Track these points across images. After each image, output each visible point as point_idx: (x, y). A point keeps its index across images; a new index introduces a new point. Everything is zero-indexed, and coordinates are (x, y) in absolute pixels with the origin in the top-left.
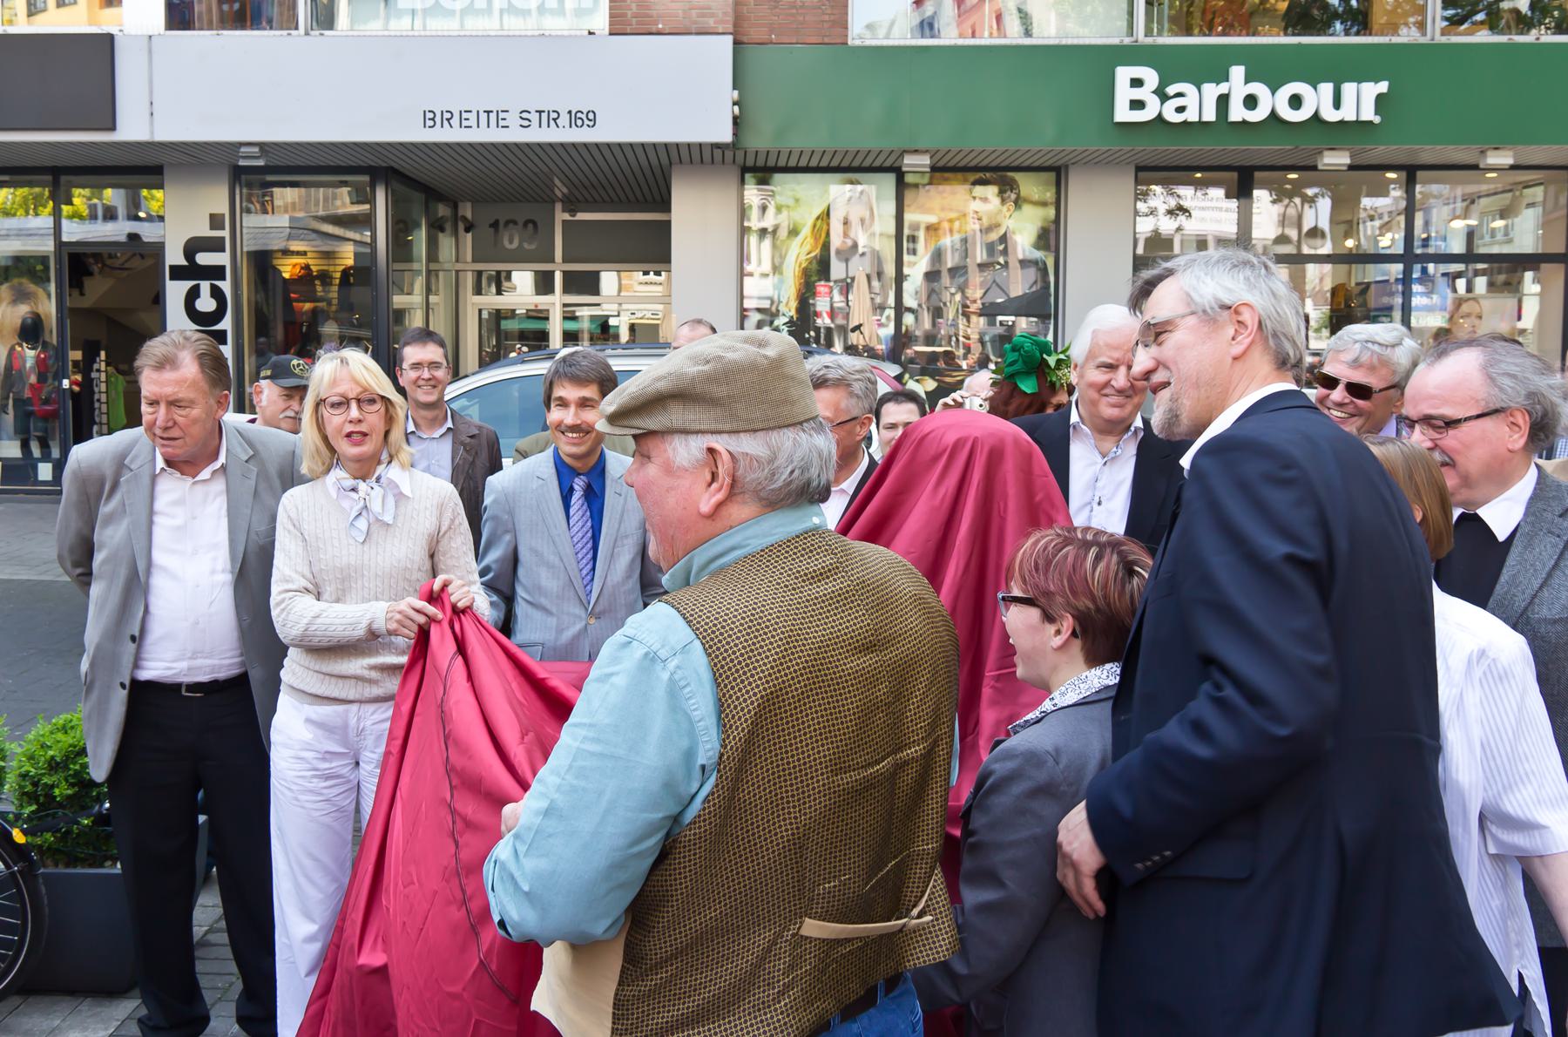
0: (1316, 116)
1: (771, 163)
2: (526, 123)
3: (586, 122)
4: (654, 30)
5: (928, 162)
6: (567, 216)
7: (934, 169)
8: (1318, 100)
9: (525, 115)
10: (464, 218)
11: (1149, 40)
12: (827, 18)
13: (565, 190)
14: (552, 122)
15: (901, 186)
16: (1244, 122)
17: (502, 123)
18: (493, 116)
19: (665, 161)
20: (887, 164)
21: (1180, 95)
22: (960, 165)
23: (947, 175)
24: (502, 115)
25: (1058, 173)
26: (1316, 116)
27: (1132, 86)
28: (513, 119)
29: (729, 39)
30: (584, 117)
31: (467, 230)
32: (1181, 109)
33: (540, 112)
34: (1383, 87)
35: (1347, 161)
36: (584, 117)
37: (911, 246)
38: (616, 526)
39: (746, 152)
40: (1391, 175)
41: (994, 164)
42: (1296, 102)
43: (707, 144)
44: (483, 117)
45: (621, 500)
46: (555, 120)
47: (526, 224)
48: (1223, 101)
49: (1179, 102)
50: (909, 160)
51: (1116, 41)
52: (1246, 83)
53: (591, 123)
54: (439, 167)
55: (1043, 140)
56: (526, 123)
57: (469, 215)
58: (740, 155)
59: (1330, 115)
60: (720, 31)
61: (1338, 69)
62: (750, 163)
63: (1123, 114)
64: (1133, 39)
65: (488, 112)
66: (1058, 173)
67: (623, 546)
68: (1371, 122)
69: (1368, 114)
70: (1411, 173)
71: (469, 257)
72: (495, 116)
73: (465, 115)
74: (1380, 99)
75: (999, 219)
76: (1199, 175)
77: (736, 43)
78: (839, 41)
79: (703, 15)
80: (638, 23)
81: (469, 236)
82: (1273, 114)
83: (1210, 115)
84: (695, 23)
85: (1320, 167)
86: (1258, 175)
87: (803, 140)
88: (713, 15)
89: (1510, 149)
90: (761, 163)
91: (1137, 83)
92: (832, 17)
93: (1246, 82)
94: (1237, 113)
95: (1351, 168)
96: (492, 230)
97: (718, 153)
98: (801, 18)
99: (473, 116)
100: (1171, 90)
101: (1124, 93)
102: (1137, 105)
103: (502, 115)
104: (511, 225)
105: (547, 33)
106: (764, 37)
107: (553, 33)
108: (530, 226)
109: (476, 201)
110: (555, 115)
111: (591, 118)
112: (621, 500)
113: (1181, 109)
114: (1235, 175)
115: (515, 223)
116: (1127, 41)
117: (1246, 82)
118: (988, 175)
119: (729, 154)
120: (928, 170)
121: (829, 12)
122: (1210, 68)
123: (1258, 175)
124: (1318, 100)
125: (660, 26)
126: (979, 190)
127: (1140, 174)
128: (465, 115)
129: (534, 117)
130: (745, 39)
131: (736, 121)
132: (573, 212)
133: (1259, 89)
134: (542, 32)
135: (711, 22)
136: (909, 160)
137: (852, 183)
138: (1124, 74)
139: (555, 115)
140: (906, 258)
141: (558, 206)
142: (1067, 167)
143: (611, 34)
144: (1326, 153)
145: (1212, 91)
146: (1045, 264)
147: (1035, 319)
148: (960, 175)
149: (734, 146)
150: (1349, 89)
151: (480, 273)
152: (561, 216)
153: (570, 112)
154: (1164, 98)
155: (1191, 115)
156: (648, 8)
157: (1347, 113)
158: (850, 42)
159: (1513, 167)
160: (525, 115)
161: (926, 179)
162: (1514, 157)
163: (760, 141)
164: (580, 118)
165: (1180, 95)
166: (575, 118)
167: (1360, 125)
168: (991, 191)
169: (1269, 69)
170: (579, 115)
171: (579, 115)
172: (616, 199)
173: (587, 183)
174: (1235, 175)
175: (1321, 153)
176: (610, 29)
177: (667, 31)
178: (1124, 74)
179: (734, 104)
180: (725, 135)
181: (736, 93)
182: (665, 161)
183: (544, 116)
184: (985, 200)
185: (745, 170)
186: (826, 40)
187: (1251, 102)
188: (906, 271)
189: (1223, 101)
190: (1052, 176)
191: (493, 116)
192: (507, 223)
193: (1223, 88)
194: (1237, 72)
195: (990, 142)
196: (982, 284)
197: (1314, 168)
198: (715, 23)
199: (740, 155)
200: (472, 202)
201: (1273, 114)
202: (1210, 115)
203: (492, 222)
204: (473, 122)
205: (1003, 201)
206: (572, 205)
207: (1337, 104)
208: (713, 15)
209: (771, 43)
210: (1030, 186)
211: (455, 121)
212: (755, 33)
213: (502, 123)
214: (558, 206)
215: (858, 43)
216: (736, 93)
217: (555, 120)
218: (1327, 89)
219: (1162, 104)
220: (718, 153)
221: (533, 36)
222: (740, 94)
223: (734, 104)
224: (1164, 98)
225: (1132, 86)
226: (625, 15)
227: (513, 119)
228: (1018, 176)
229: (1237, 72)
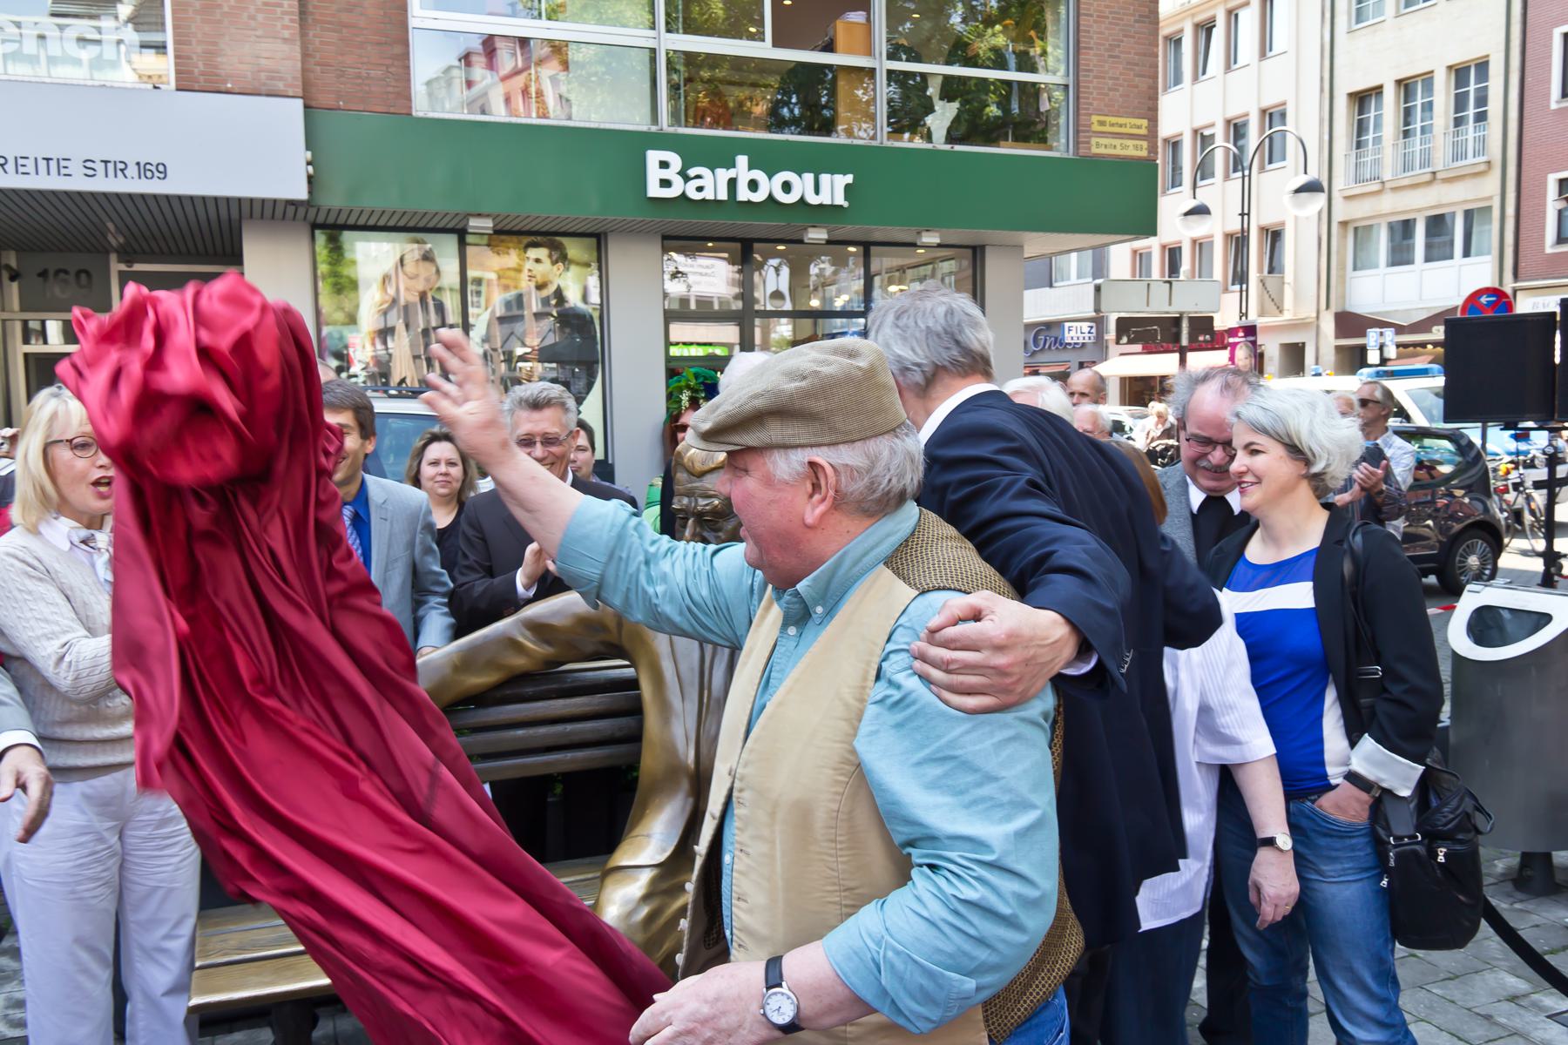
0: (802, 199)
1: (341, 221)
2: (91, 172)
3: (157, 174)
4: (223, 89)
5: (491, 225)
6: (123, 267)
7: (499, 232)
8: (803, 186)
9: (88, 164)
10: (8, 267)
11: (672, 130)
12: (391, 89)
13: (121, 240)
14: (119, 173)
15: (462, 244)
16: (749, 202)
17: (63, 171)
18: (53, 164)
19: (235, 214)
20: (450, 226)
21: (698, 177)
22: (515, 229)
23: (503, 237)
24: (63, 163)
25: (598, 239)
26: (802, 199)
27: (661, 168)
28: (76, 168)
29: (299, 103)
30: (153, 169)
31: (12, 278)
32: (700, 189)
33: (106, 162)
34: (849, 178)
35: (825, 236)
36: (153, 169)
37: (475, 299)
38: (386, 550)
39: (319, 210)
40: (852, 249)
41: (544, 229)
42: (787, 187)
43: (281, 200)
44: (42, 164)
45: (388, 523)
46: (122, 170)
47: (78, 273)
48: (732, 183)
49: (698, 183)
50: (474, 223)
51: (644, 128)
52: (749, 170)
53: (162, 176)
54: (22, 214)
55: (589, 210)
56: (91, 172)
57: (13, 263)
58: (312, 212)
59: (813, 199)
60: (291, 94)
61: (818, 163)
62: (320, 220)
63: (654, 190)
64: (659, 127)
65: (48, 160)
66: (598, 239)
67: (394, 569)
68: (841, 206)
69: (840, 200)
70: (867, 246)
71: (16, 305)
72: (60, 165)
73: (21, 162)
74: (847, 187)
75: (551, 277)
76: (710, 244)
77: (306, 107)
78: (403, 112)
79: (272, 78)
80: (205, 81)
81: (15, 285)
82: (771, 197)
83: (723, 195)
84: (265, 84)
85: (806, 241)
86: (756, 245)
87: (373, 201)
88: (281, 79)
89: (936, 231)
90: (331, 220)
91: (664, 165)
92: (396, 90)
93: (750, 169)
94: (744, 194)
95: (829, 242)
96: (41, 279)
97: (291, 209)
98: (367, 88)
99: (30, 164)
100: (692, 172)
101: (654, 174)
102: (665, 183)
103: (63, 163)
104: (62, 275)
105: (108, 84)
106: (332, 103)
107: (116, 85)
108: (83, 276)
109: (21, 249)
110: (122, 166)
111: (162, 171)
112: (388, 523)
113: (700, 189)
114: (738, 245)
115: (66, 272)
116: (654, 129)
117: (750, 169)
118: (539, 238)
119: (301, 211)
120: (491, 232)
121: (393, 84)
122: (720, 156)
123: (756, 245)
124: (803, 186)
125: (229, 85)
126: (533, 253)
127: (665, 242)
128: (21, 162)
129: (100, 167)
130: (313, 103)
131: (310, 179)
132: (129, 262)
133: (759, 175)
134: (102, 83)
135: (280, 85)
136: (474, 223)
137: (418, 242)
138: (654, 157)
139: (122, 166)
140: (471, 310)
141: (113, 257)
142: (606, 234)
143: (178, 90)
144: (810, 230)
145: (723, 175)
146: (591, 317)
147: (554, 365)
148: (515, 238)
149: (307, 204)
150: (825, 178)
151: (25, 323)
152: (116, 267)
153: (138, 164)
154: (687, 179)
155: (708, 194)
156: (216, 67)
157: (824, 198)
158: (414, 114)
159: (939, 246)
160: (88, 164)
161: (485, 240)
162: (940, 238)
163: (334, 200)
164: (160, 172)
165: (698, 177)
166: (144, 170)
167: (834, 208)
168: (542, 253)
169: (766, 160)
170: (148, 167)
171: (148, 167)
172: (183, 249)
173: (147, 234)
174: (738, 245)
175: (805, 229)
176: (177, 85)
177: (237, 91)
178: (654, 157)
179: (309, 163)
180: (301, 193)
181: (309, 154)
182: (235, 214)
183: (111, 166)
184: (538, 261)
185: (315, 226)
186: (392, 110)
187: (753, 185)
188: (471, 320)
189: (732, 183)
190: (593, 241)
191: (53, 164)
192: (58, 272)
193: (732, 173)
194: (742, 160)
195: (542, 209)
196: (538, 333)
197: (801, 242)
198: (285, 85)
199: (312, 212)
200: (17, 251)
201: (771, 197)
202: (723, 195)
203: (39, 271)
204: (31, 168)
205: (554, 263)
206: (128, 255)
207: (817, 192)
208: (281, 79)
209: (340, 109)
210: (574, 249)
211: (10, 167)
212: (323, 99)
213: (63, 171)
214: (113, 257)
215: (421, 114)
216: (309, 154)
217: (122, 170)
218: (809, 177)
219: (686, 182)
220: (291, 209)
221: (93, 86)
222: (313, 155)
223: (309, 163)
224: (687, 179)
225: (661, 168)
226: (191, 72)
227: (76, 168)
228: (565, 241)
229: (742, 160)
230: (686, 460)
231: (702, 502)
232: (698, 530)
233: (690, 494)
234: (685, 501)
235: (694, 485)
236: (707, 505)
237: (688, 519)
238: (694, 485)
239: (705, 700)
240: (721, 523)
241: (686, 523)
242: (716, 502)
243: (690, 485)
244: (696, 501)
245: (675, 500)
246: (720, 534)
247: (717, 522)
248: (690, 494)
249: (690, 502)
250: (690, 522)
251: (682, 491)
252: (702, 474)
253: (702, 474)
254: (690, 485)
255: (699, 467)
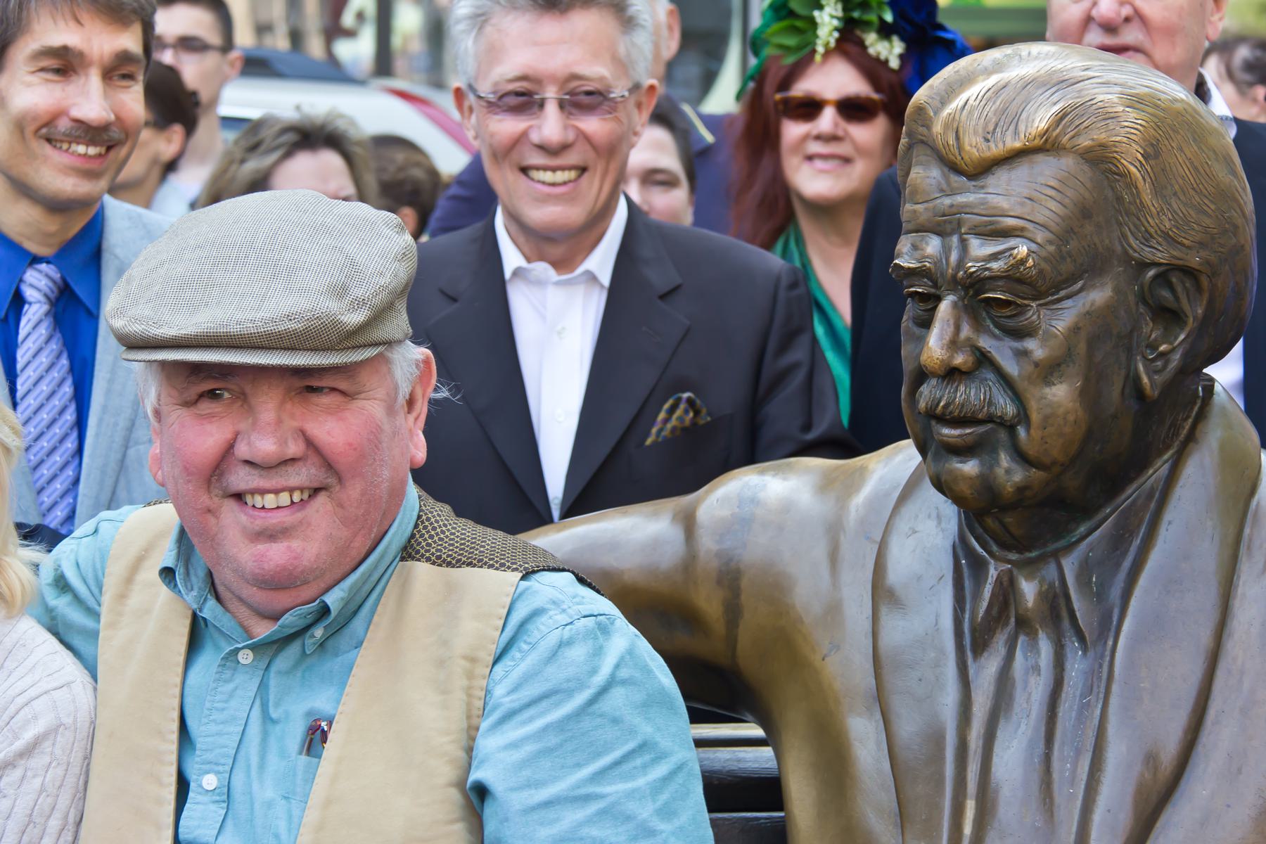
230: (937, 128)
231: (980, 248)
232: (966, 331)
233: (944, 226)
234: (933, 245)
235: (960, 199)
236: (995, 257)
237: (938, 299)
238: (960, 199)
239: (968, 829)
240: (1034, 312)
241: (934, 308)
242: (1022, 250)
243: (947, 201)
244: (964, 244)
245: (904, 244)
246: (1031, 344)
247: (1023, 309)
248: (944, 226)
249: (946, 250)
250: (945, 307)
251: (923, 218)
252: (983, 170)
253: (983, 170)
254: (947, 201)
255: (975, 147)
